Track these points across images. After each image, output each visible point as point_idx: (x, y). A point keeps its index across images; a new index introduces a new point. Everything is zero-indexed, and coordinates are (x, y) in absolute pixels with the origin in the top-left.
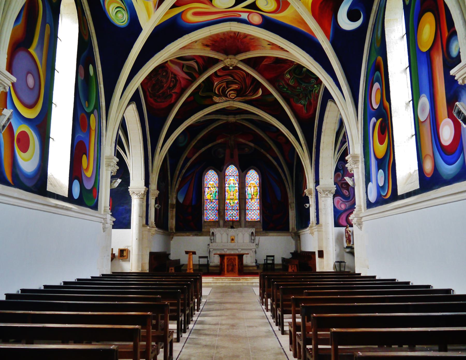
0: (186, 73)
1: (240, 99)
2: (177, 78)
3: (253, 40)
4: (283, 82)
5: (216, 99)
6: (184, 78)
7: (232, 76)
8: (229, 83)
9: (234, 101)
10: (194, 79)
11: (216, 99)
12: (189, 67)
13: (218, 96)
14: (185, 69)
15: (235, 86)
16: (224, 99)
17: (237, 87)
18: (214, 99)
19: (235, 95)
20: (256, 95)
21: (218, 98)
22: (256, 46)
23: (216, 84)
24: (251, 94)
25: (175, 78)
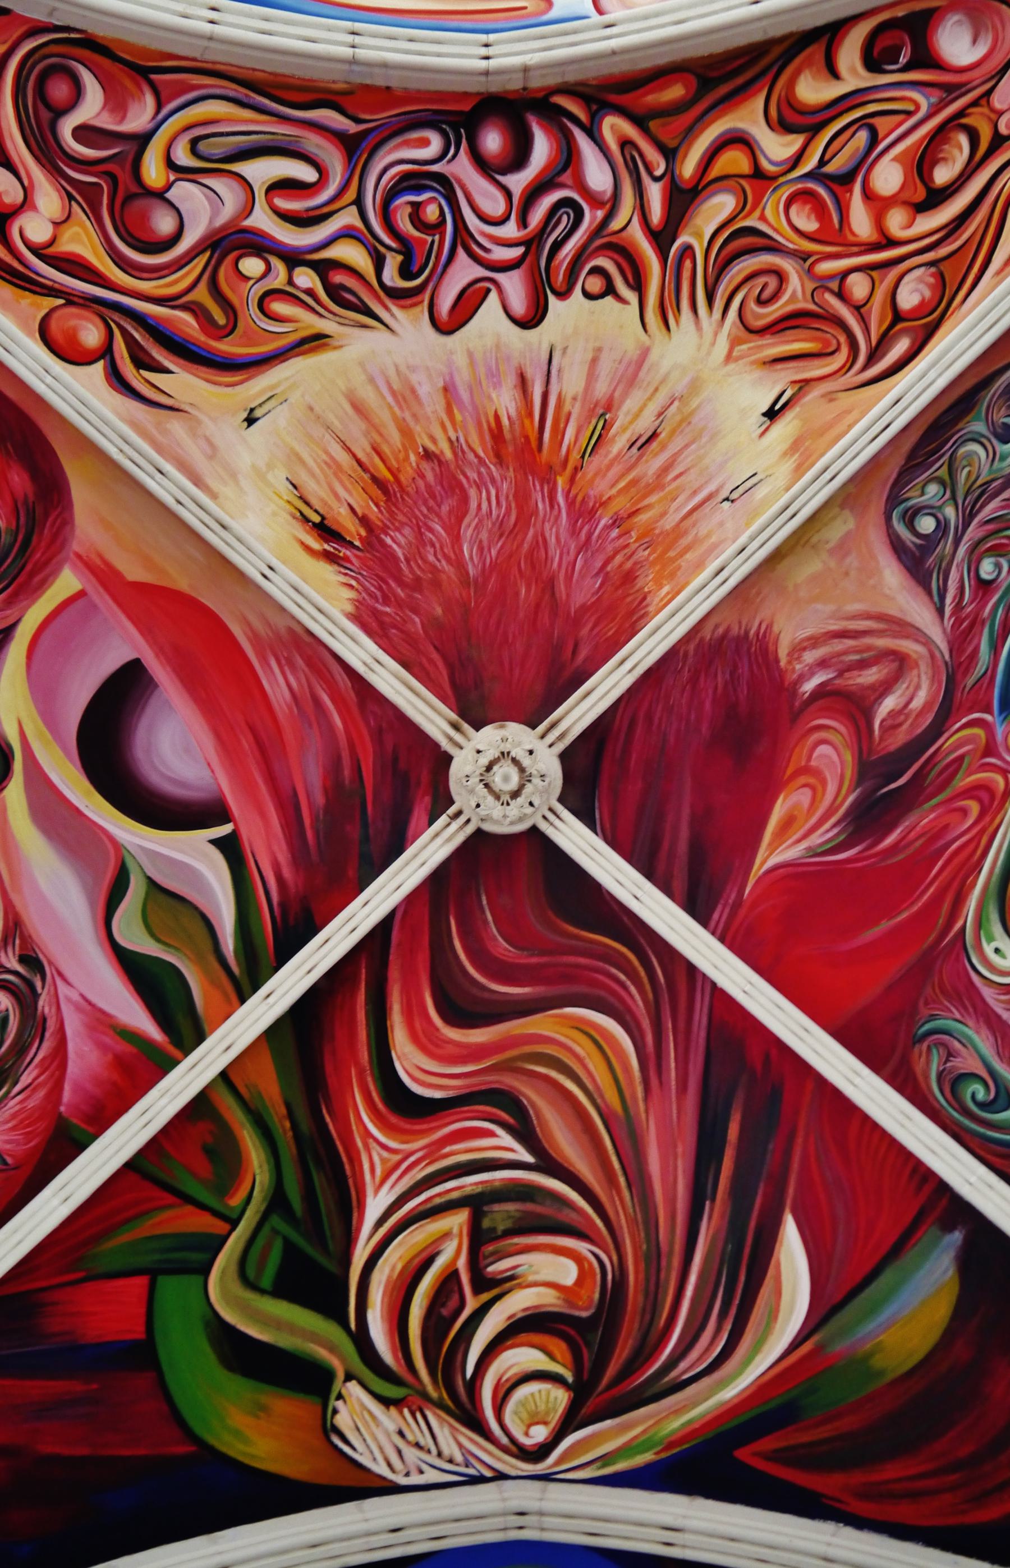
0: (133, 967)
1: (608, 1437)
2: (43, 1003)
3: (652, 464)
4: (983, 1043)
5: (367, 1426)
6: (100, 1021)
7: (525, 1131)
8: (500, 1221)
9: (545, 1478)
10: (186, 1030)
11: (367, 1426)
12: (169, 904)
13: (395, 1389)
14: (131, 931)
15: (546, 1273)
16: (450, 1437)
17: (568, 1273)
18: (343, 1420)
19: (560, 1398)
20: (757, 1348)
21: (389, 1420)
22: (678, 532)
23: (376, 1204)
24: (710, 1343)
25: (25, 998)
